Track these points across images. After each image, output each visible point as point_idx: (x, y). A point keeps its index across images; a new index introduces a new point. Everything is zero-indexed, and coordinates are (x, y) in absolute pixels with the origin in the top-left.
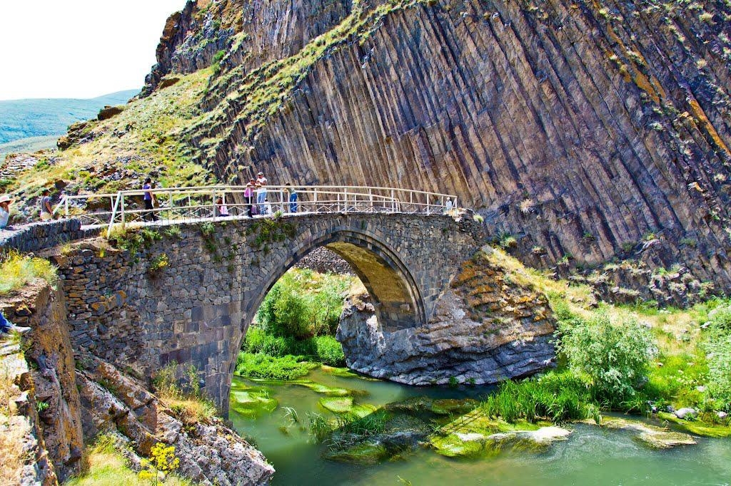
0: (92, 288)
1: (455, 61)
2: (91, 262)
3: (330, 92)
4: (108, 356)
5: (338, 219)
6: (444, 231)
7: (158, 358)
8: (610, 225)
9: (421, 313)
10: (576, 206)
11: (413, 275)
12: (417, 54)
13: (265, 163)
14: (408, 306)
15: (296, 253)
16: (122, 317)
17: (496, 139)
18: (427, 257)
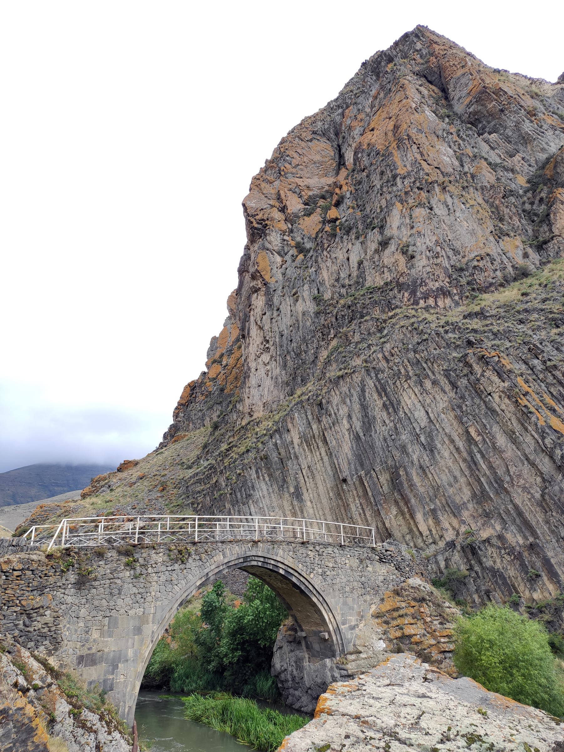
0: (24, 588)
1: (395, 412)
2: (28, 569)
3: (296, 441)
4: (29, 646)
6: (361, 561)
7: (75, 658)
9: (340, 642)
16: (46, 615)
18: (343, 585)
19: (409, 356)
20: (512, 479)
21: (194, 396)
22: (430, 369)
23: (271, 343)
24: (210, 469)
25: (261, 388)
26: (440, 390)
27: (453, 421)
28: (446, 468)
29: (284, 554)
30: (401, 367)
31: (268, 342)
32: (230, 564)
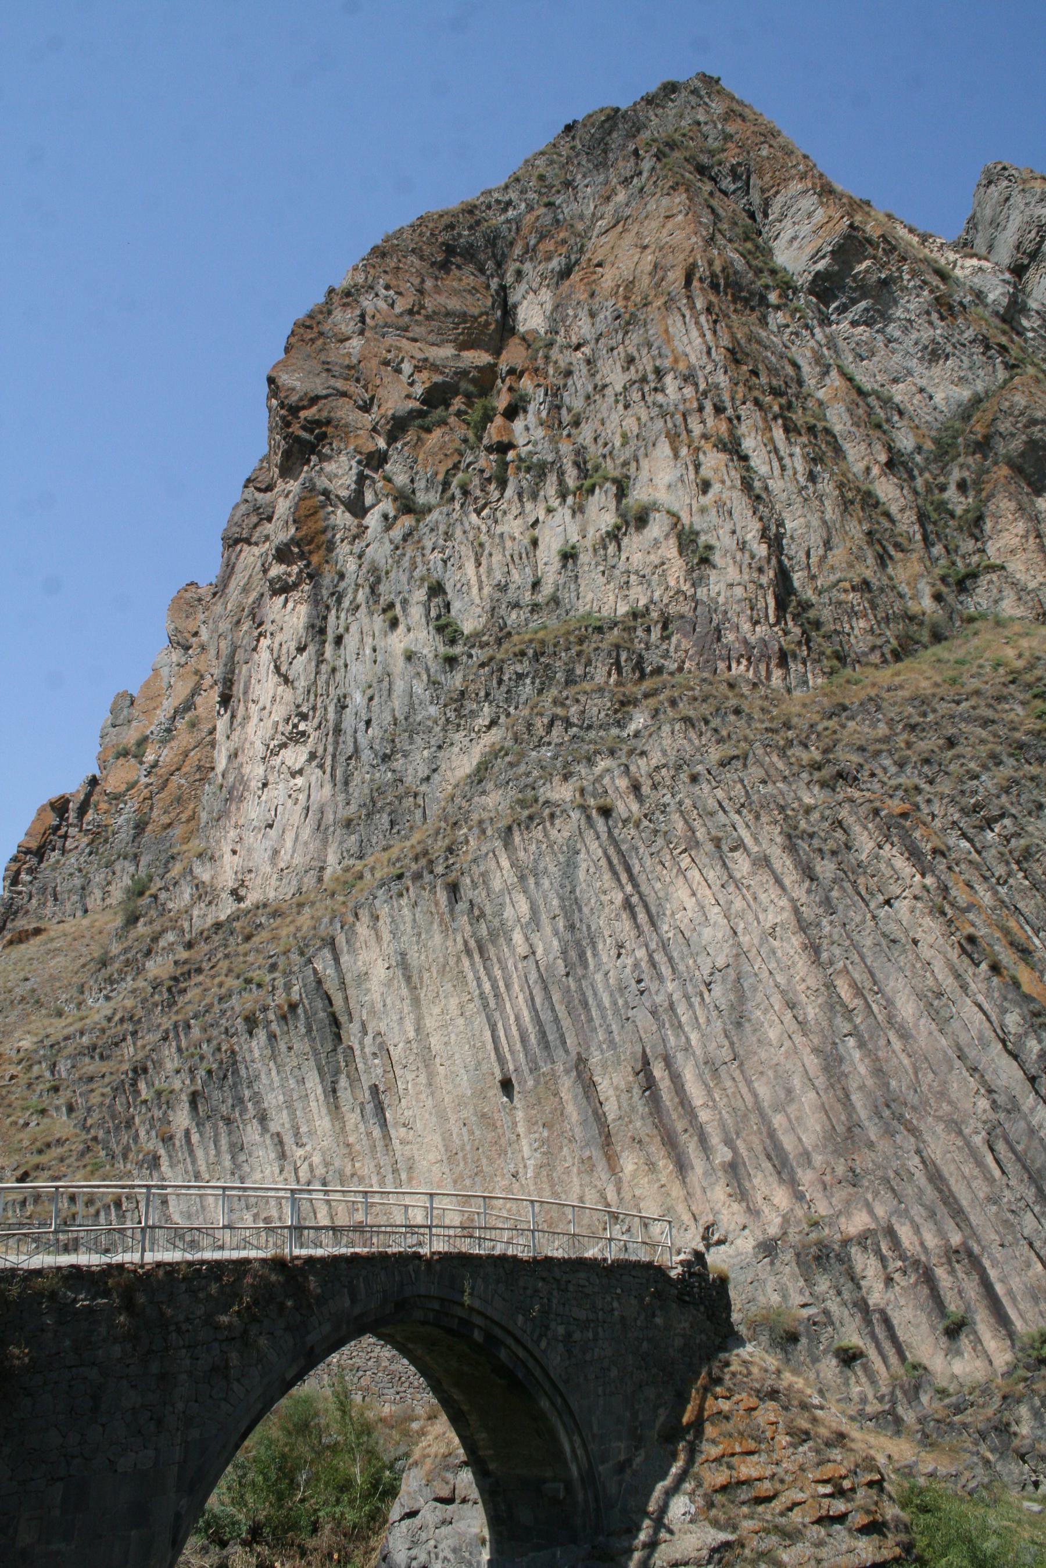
1: (653, 923)
5: (411, 1267)
8: (999, 1288)
10: (922, 1244)
13: (221, 1124)
14: (562, 1486)
15: (312, 1348)
17: (744, 1090)
20: (926, 1103)
21: (62, 832)
23: (316, 722)
25: (272, 833)
27: (796, 956)
30: (676, 817)
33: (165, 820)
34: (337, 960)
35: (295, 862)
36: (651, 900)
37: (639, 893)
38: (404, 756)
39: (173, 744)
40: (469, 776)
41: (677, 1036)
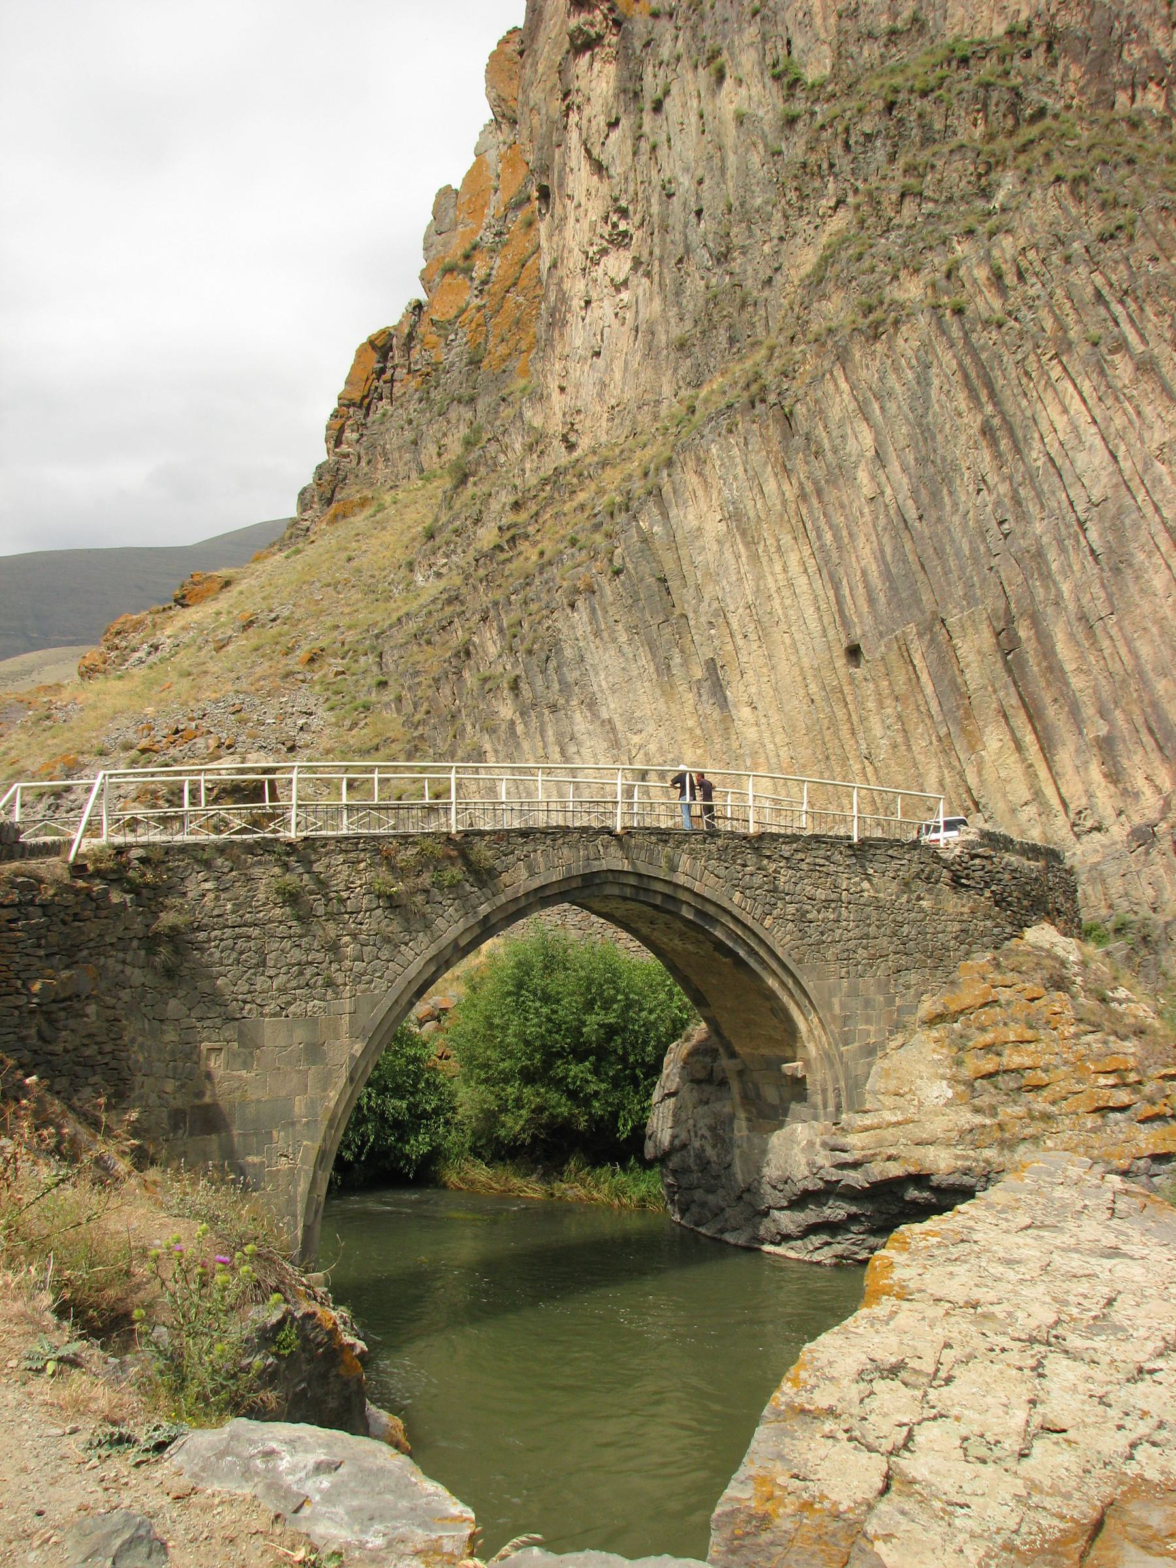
1: (1018, 451)
6: (906, 885)
7: (165, 1115)
11: (809, 986)
12: (924, 431)
13: (546, 712)
15: (486, 917)
17: (1123, 651)
19: (1073, 277)
21: (387, 376)
22: (1132, 321)
23: (637, 219)
24: (449, 601)
25: (600, 362)
26: (1158, 390)
28: (1155, 622)
29: (693, 866)
30: (1044, 313)
31: (624, 213)
32: (548, 893)
33: (502, 350)
34: (665, 515)
35: (626, 396)
36: (1017, 421)
37: (1002, 414)
38: (744, 254)
39: (505, 251)
40: (808, 276)
41: (1047, 588)
